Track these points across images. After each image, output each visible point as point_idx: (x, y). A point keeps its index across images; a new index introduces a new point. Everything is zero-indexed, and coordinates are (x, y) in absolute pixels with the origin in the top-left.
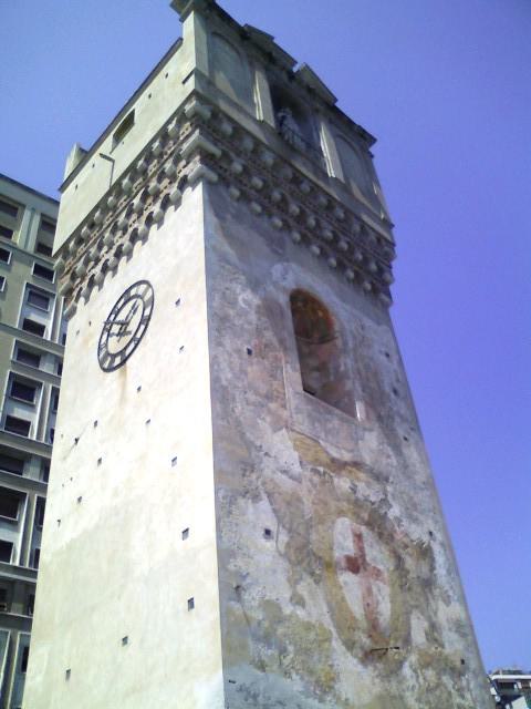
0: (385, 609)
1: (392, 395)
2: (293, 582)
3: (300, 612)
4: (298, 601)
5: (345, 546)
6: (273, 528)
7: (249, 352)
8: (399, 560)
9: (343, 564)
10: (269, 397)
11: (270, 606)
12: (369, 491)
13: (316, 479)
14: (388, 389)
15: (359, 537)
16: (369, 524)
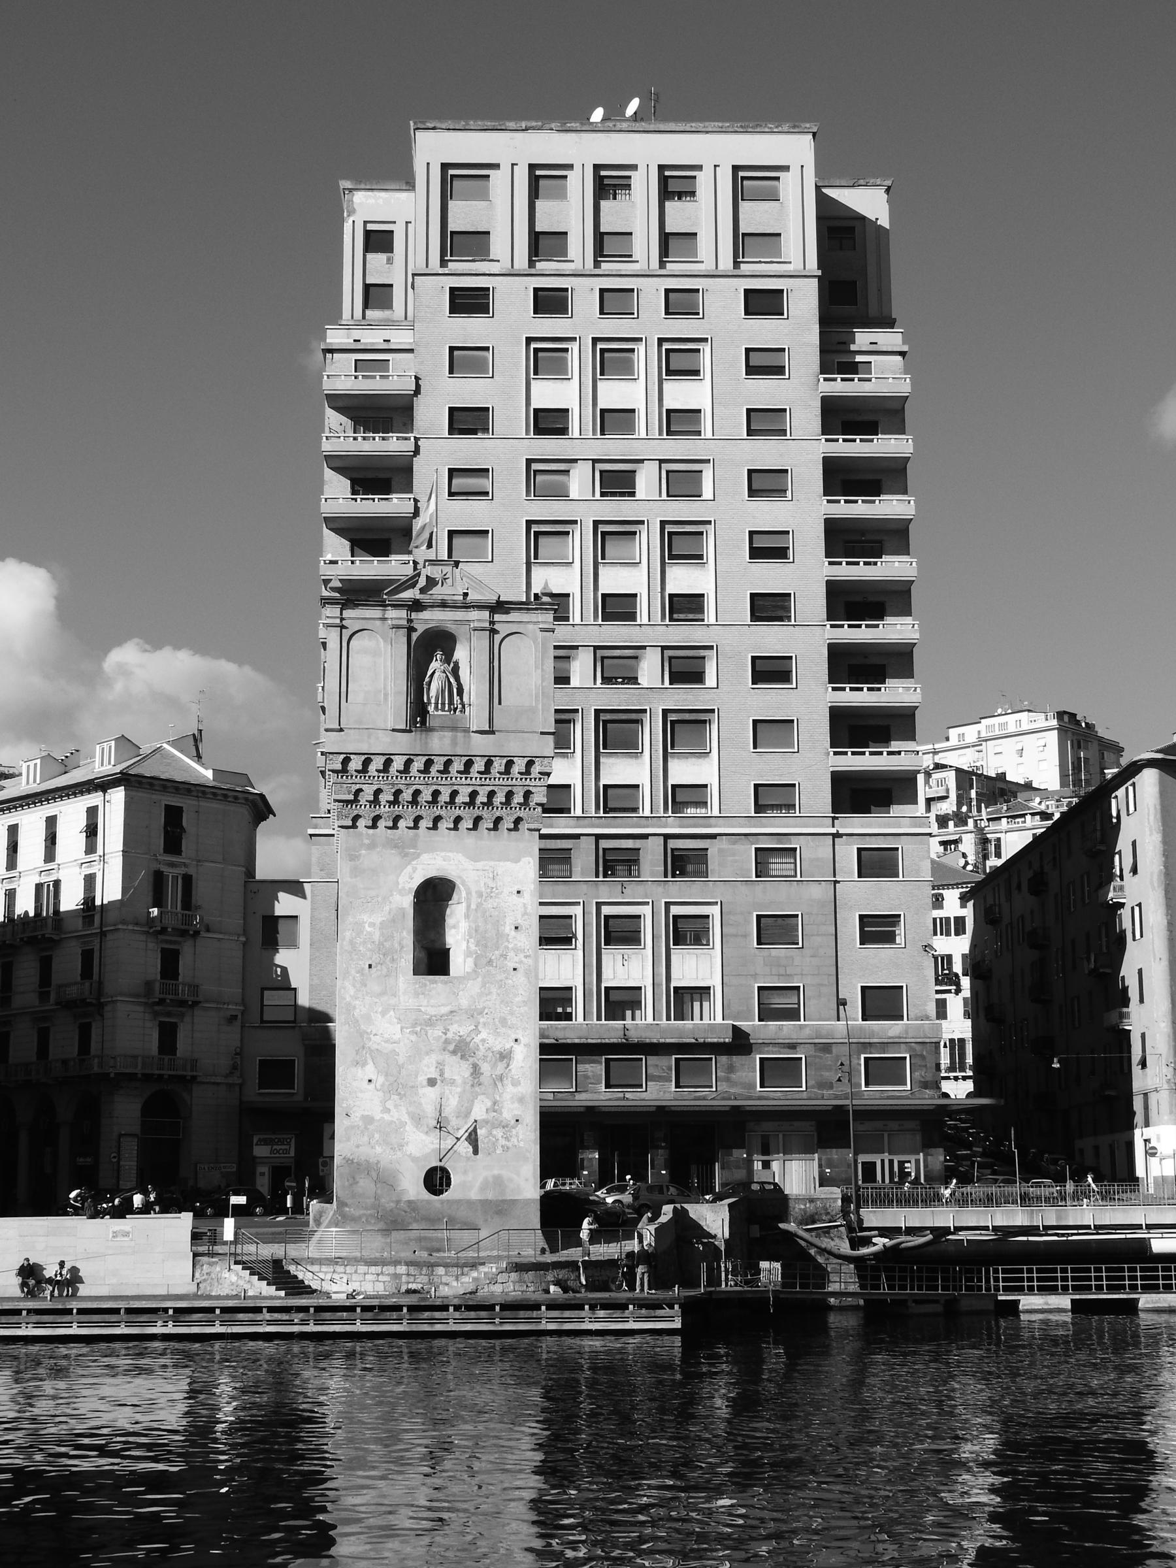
1: (513, 933)
2: (384, 1102)
3: (386, 1117)
4: (388, 1111)
6: (373, 1077)
7: (370, 966)
9: (425, 1083)
10: (383, 993)
11: (368, 1120)
12: (460, 1029)
13: (413, 1038)
14: (508, 929)
15: (440, 1066)
16: (454, 1052)
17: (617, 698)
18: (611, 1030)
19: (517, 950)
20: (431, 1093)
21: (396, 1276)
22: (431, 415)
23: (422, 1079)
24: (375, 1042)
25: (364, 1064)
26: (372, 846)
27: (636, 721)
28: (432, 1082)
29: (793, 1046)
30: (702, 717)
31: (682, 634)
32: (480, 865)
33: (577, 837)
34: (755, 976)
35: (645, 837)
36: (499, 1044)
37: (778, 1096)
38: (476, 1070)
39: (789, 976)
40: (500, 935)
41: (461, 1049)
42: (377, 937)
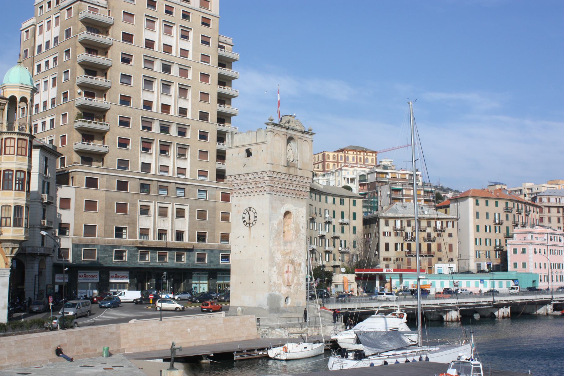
0: (291, 278)
5: (286, 269)
8: (295, 267)
11: (275, 283)
12: (292, 256)
14: (301, 227)
17: (164, 138)
18: (162, 243)
19: (303, 234)
20: (286, 275)
21: (312, 330)
22: (116, 33)
23: (285, 271)
24: (276, 260)
25: (274, 266)
26: (275, 200)
27: (169, 146)
28: (287, 272)
29: (204, 250)
30: (185, 147)
31: (181, 121)
32: (296, 208)
33: (152, 180)
34: (196, 229)
35: (170, 183)
36: (299, 261)
37: (200, 265)
38: (295, 270)
39: (204, 229)
40: (299, 230)
41: (292, 262)
42: (276, 228)
